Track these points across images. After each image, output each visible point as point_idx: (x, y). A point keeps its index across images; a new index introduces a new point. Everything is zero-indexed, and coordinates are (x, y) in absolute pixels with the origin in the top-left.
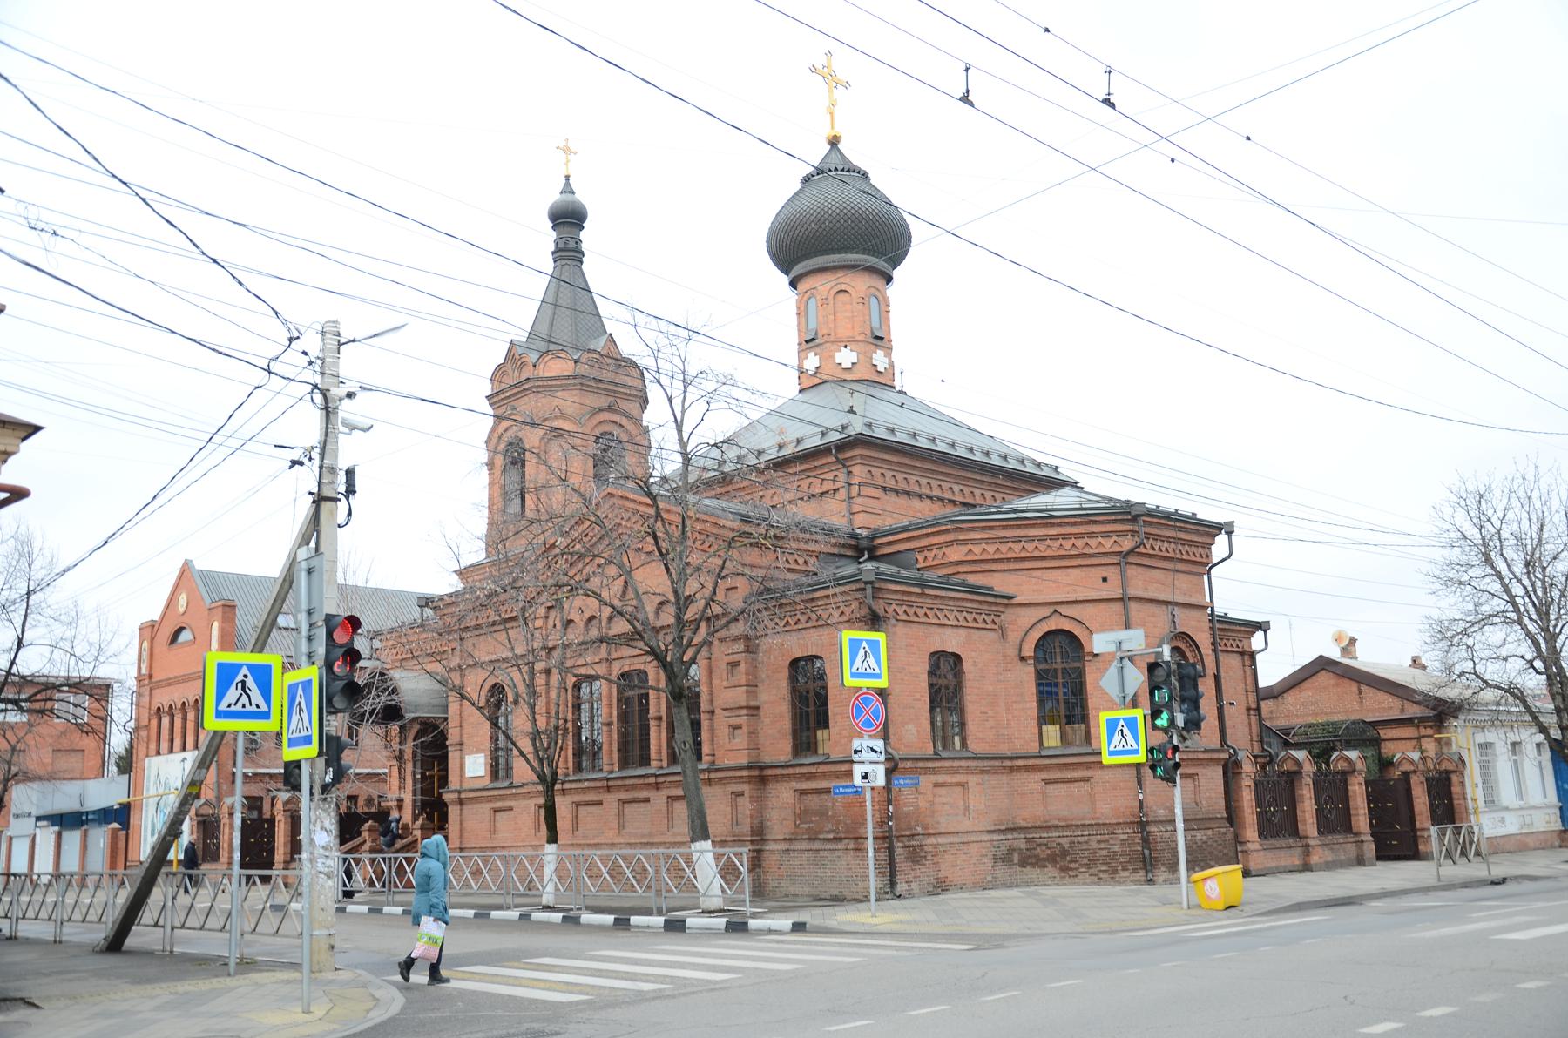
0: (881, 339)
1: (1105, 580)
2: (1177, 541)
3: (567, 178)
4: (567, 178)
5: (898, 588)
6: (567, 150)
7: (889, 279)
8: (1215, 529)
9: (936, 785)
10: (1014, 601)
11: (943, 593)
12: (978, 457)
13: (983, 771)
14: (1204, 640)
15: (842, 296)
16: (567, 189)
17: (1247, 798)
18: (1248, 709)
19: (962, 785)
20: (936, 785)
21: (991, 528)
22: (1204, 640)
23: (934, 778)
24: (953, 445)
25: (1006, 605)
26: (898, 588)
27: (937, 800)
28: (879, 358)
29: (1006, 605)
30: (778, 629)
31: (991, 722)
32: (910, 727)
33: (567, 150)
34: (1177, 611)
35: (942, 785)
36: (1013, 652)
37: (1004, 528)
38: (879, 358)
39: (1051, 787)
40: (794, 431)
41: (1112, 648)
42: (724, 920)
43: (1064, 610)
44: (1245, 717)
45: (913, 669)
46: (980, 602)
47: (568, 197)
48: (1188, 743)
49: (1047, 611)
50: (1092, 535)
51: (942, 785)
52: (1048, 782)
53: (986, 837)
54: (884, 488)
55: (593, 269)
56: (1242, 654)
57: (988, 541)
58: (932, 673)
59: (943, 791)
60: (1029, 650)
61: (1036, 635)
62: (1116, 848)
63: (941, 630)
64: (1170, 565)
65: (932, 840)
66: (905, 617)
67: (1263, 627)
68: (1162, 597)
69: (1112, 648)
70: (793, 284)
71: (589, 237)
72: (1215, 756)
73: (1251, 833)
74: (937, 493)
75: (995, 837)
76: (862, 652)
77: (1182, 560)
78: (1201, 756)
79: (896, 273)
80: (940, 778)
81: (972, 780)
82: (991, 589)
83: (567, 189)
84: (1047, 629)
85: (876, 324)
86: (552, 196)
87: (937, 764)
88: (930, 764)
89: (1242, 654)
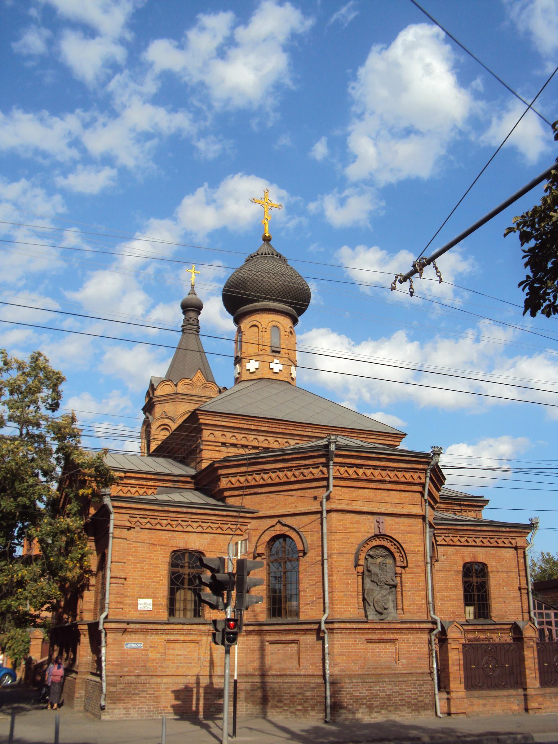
0: (279, 352)
2: (383, 468)
9: (169, 641)
15: (255, 329)
16: (193, 292)
17: (455, 656)
18: (520, 589)
20: (169, 641)
34: (382, 518)
35: (176, 642)
43: (285, 520)
44: (517, 594)
47: (194, 296)
48: (383, 617)
49: (275, 520)
50: (306, 466)
51: (176, 642)
56: (516, 548)
58: (173, 564)
60: (261, 549)
61: (267, 537)
63: (184, 535)
64: (381, 486)
65: (154, 680)
73: (457, 685)
77: (390, 482)
80: (172, 638)
84: (274, 534)
88: (159, 627)
89: (516, 548)
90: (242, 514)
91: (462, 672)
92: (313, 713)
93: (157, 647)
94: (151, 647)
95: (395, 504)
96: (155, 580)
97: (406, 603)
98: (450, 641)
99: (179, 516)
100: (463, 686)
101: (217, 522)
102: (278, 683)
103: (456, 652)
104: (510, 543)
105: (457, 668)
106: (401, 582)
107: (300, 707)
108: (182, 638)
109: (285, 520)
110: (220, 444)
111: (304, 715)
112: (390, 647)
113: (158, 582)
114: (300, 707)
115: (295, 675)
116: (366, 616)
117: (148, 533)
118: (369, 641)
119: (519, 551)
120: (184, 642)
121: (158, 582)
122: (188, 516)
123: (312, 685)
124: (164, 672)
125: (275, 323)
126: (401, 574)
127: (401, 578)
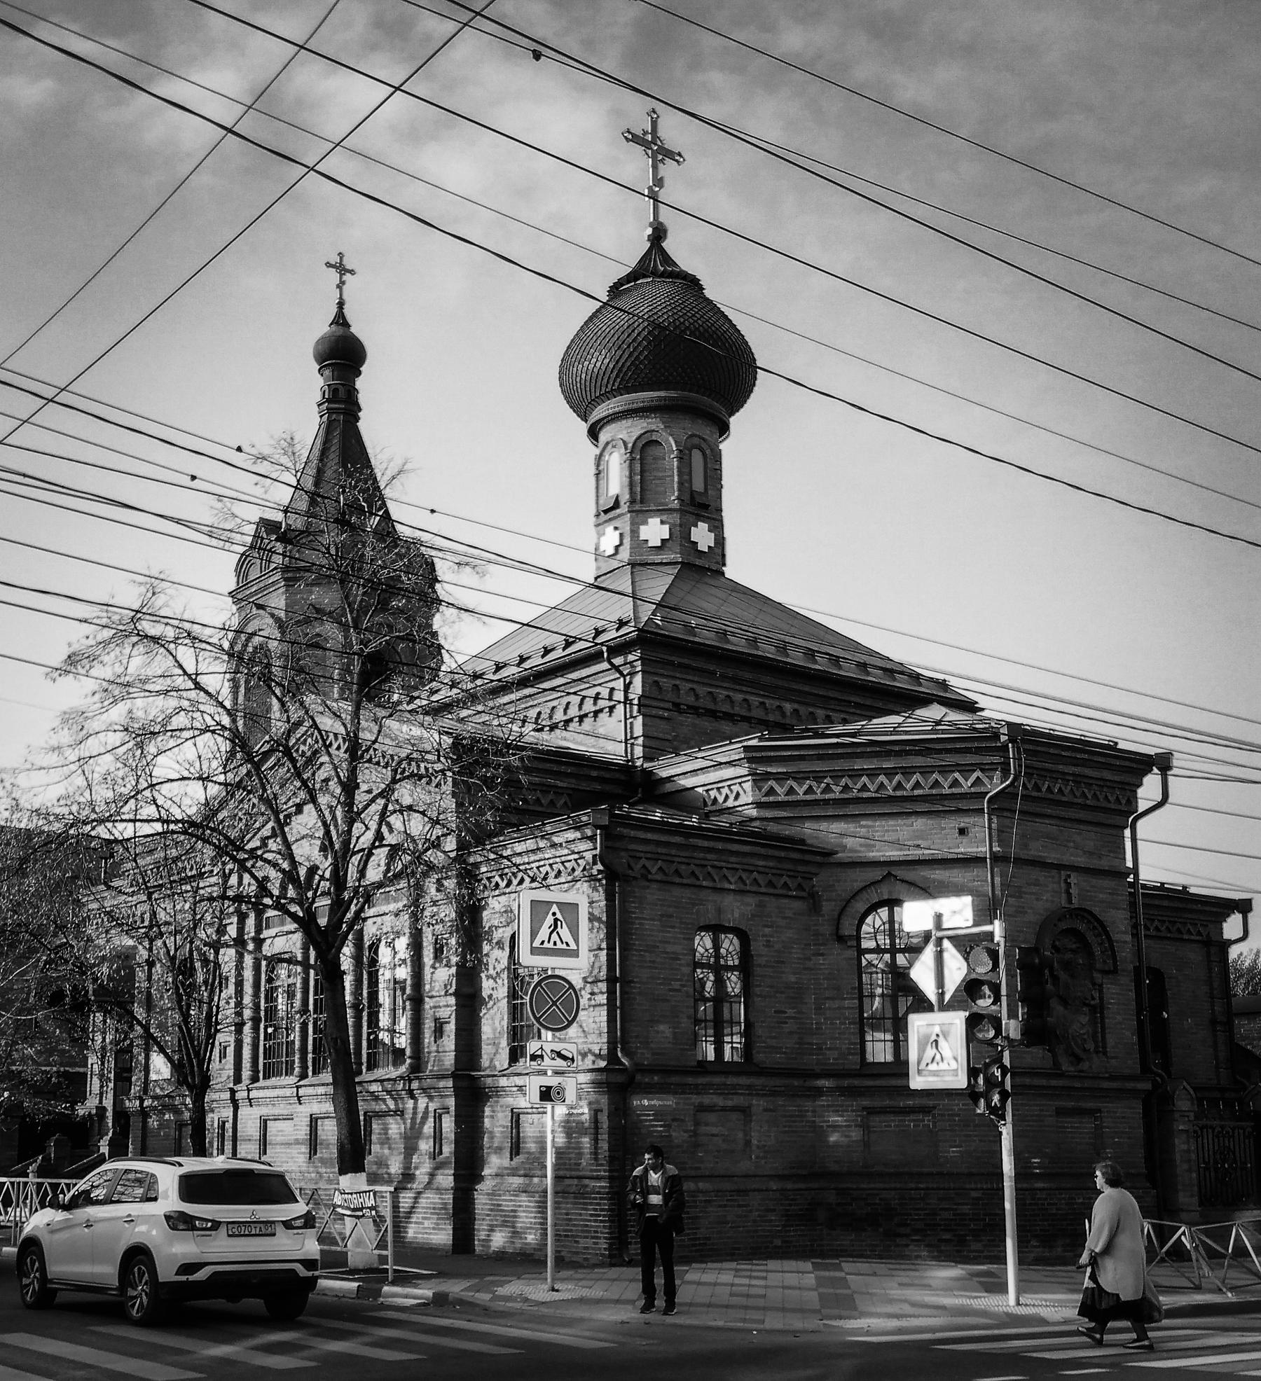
1: (962, 832)
3: (341, 305)
4: (341, 305)
5: (649, 836)
6: (341, 269)
7: (724, 429)
8: (1141, 764)
10: (832, 860)
11: (720, 846)
12: (821, 665)
13: (774, 1093)
14: (1119, 921)
16: (340, 320)
18: (1214, 1022)
19: (745, 1111)
20: (701, 1109)
21: (802, 758)
22: (1119, 921)
23: (696, 1099)
24: (754, 642)
25: (821, 865)
26: (649, 836)
27: (703, 1129)
28: (702, 535)
29: (821, 865)
30: (512, 888)
31: (789, 1027)
32: (661, 1027)
33: (341, 269)
35: (711, 1109)
36: (826, 929)
37: (820, 757)
38: (702, 535)
39: (876, 1120)
40: (581, 627)
41: (929, 925)
42: (356, 1284)
43: (899, 872)
45: (670, 948)
46: (779, 859)
49: (877, 874)
52: (871, 1111)
53: (774, 1185)
54: (677, 705)
55: (368, 426)
57: (799, 777)
59: (712, 1117)
62: (966, 1209)
66: (659, 877)
67: (1244, 907)
68: (1052, 857)
69: (929, 925)
70: (593, 433)
71: (369, 385)
72: (1130, 1085)
74: (757, 713)
75: (789, 1186)
76: (550, 920)
78: (1106, 1085)
79: (733, 421)
80: (707, 1100)
81: (758, 1104)
82: (802, 842)
83: (340, 320)
85: (698, 485)
86: (322, 327)
87: (701, 1080)
90: (808, 857)
91: (1194, 1175)
92: (975, 1246)
93: (682, 1121)
94: (674, 1120)
95: (897, 843)
96: (676, 985)
97: (1111, 1041)
98: (1177, 1115)
99: (709, 856)
100: (1195, 1200)
101: (767, 870)
102: (944, 1189)
103: (1184, 1136)
104: (1199, 934)
105: (1185, 1166)
106: (1101, 999)
107: (947, 1236)
108: (720, 1101)
109: (899, 872)
110: (670, 706)
111: (958, 1251)
112: (1088, 1125)
113: (679, 990)
114: (947, 1236)
115: (931, 1174)
116: (1056, 1064)
117: (659, 890)
118: (1060, 1112)
119: (1213, 950)
120: (724, 1109)
121: (679, 990)
122: (723, 858)
123: (974, 1194)
124: (699, 1168)
125: (696, 441)
126: (1101, 985)
127: (1101, 992)
